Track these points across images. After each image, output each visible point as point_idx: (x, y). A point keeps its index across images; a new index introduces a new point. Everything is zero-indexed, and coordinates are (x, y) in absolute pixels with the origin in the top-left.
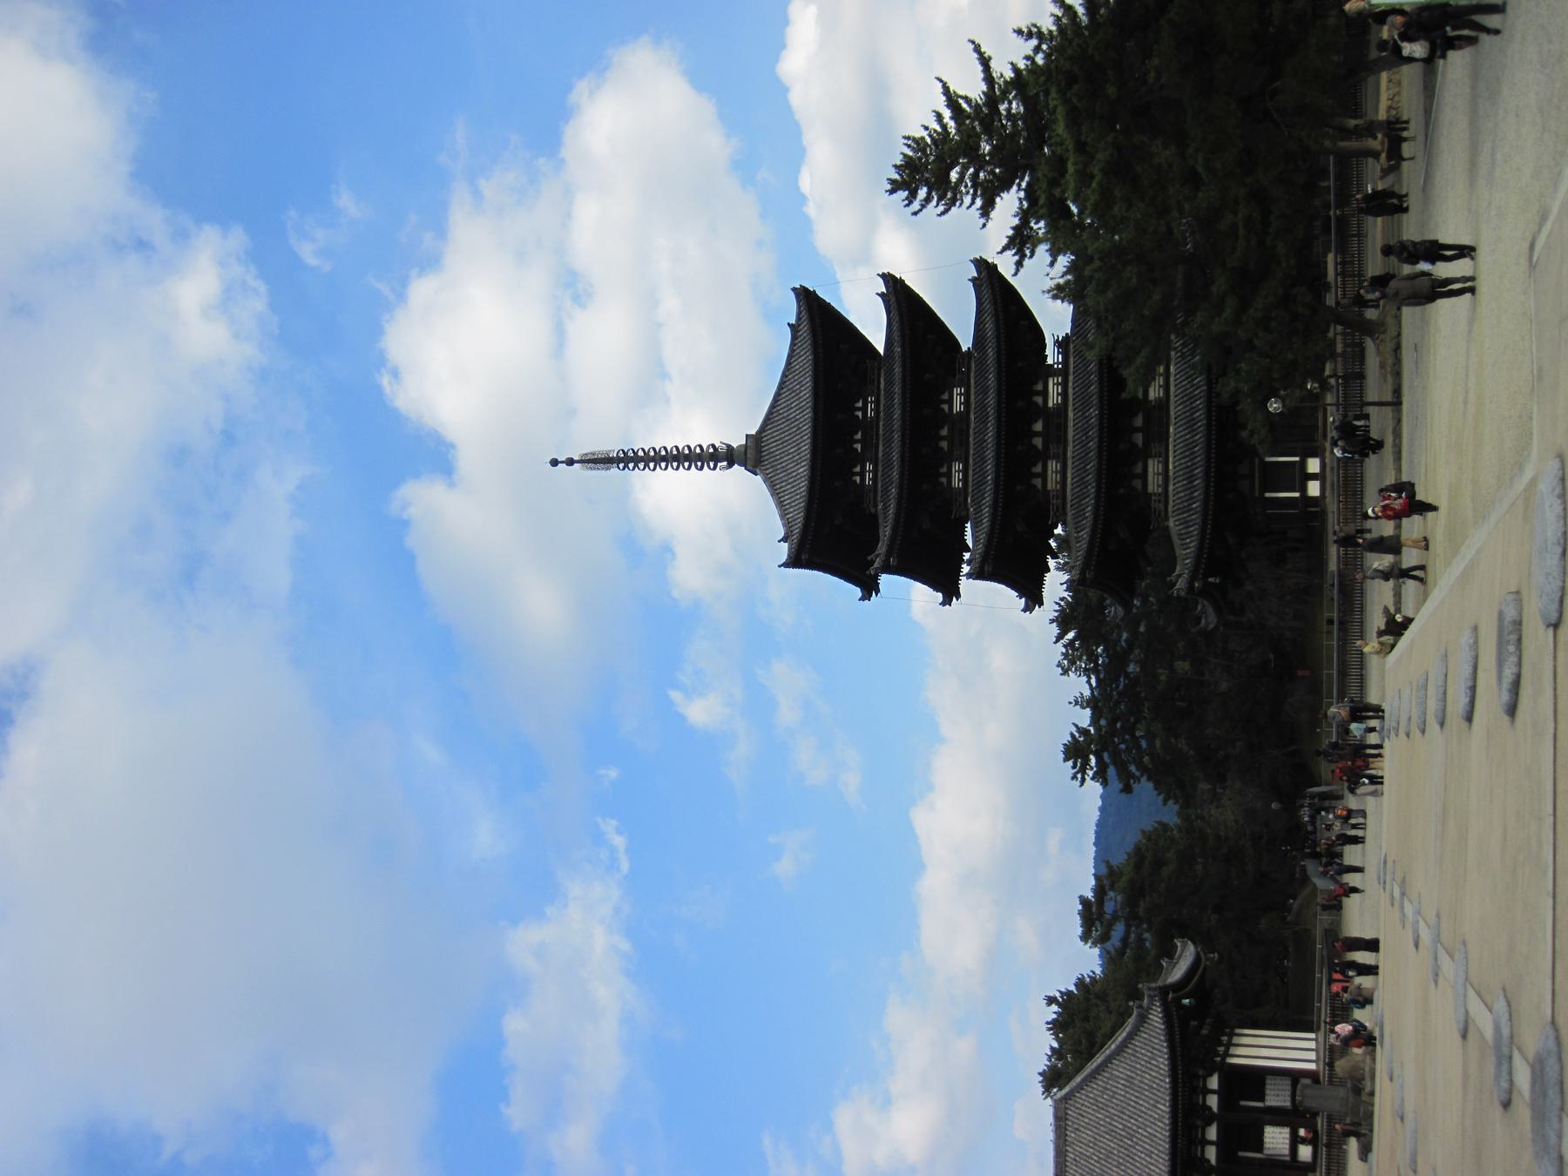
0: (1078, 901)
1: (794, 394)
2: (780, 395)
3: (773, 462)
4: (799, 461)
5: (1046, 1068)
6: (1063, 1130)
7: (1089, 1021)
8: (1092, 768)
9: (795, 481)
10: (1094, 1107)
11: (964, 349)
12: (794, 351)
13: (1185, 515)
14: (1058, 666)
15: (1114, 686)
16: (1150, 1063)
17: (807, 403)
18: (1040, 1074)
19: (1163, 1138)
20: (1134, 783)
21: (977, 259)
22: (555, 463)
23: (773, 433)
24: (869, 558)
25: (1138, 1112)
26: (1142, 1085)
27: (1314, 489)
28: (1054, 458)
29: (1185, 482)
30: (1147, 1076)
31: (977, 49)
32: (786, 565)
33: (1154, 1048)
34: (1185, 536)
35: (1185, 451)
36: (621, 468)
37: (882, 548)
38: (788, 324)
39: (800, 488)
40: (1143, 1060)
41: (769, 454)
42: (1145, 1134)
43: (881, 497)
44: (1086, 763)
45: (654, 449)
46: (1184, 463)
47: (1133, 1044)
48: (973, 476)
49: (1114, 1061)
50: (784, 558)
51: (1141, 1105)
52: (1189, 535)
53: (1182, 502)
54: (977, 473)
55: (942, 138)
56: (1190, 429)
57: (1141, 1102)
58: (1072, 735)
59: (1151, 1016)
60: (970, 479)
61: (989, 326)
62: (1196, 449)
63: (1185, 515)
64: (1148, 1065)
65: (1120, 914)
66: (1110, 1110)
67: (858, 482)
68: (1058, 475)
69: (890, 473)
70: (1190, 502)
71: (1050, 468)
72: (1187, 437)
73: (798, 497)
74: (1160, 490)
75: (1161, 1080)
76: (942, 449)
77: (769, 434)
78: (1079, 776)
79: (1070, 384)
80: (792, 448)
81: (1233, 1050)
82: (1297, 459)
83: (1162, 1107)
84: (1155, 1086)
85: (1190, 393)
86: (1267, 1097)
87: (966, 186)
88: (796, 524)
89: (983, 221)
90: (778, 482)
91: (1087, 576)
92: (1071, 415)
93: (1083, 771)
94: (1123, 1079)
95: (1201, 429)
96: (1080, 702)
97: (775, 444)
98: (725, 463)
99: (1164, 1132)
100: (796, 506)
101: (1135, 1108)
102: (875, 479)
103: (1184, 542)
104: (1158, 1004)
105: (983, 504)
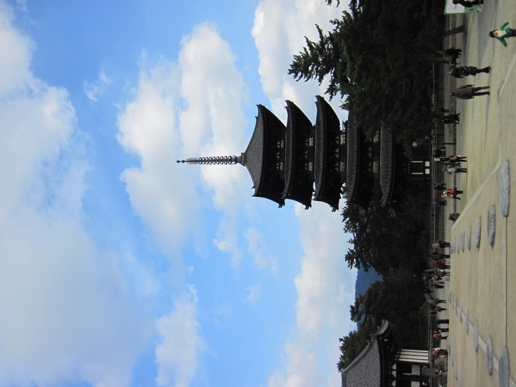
0: (350, 307)
1: (257, 140)
2: (252, 140)
3: (250, 162)
4: (259, 162)
5: (339, 362)
6: (345, 383)
7: (353, 346)
8: (354, 263)
9: (257, 168)
10: (355, 375)
11: (313, 125)
12: (257, 125)
13: (385, 180)
14: (344, 230)
15: (362, 236)
16: (374, 361)
17: (261, 143)
18: (337, 364)
19: (378, 385)
20: (369, 268)
22: (178, 162)
23: (250, 152)
24: (282, 194)
25: (370, 377)
26: (371, 368)
27: (427, 171)
28: (342, 161)
29: (385, 169)
30: (373, 365)
31: (318, 27)
32: (254, 196)
33: (375, 356)
34: (385, 187)
35: (385, 159)
36: (200, 164)
37: (286, 190)
38: (255, 117)
39: (259, 171)
40: (371, 359)
41: (249, 159)
42: (372, 384)
43: (286, 174)
44: (353, 261)
45: (211, 157)
46: (385, 163)
47: (368, 354)
48: (316, 167)
49: (361, 360)
50: (254, 193)
51: (371, 374)
52: (387, 187)
53: (384, 176)
54: (317, 166)
55: (306, 56)
56: (387, 152)
57: (370, 373)
58: (348, 252)
59: (374, 345)
60: (315, 168)
61: (321, 118)
62: (389, 158)
63: (385, 180)
64: (373, 361)
65: (364, 311)
66: (360, 376)
67: (278, 168)
68: (344, 167)
69: (289, 166)
70: (387, 176)
71: (341, 166)
72: (386, 154)
73: (258, 173)
74: (377, 172)
75: (377, 366)
76: (306, 158)
77: (249, 153)
78: (350, 266)
79: (348, 137)
80: (256, 157)
81: (401, 356)
82: (422, 162)
83: (377, 375)
84: (375, 368)
85: (387, 140)
86: (412, 372)
87: (314, 72)
88: (257, 182)
89: (319, 83)
90: (252, 168)
91: (353, 200)
92: (348, 147)
93: (352, 265)
94: (365, 366)
95: (391, 152)
96: (351, 242)
97: (251, 156)
98: (234, 162)
99: (378, 384)
100: (257, 176)
101: (368, 375)
102: (283, 168)
103: (385, 189)
104: (376, 341)
105: (319, 176)
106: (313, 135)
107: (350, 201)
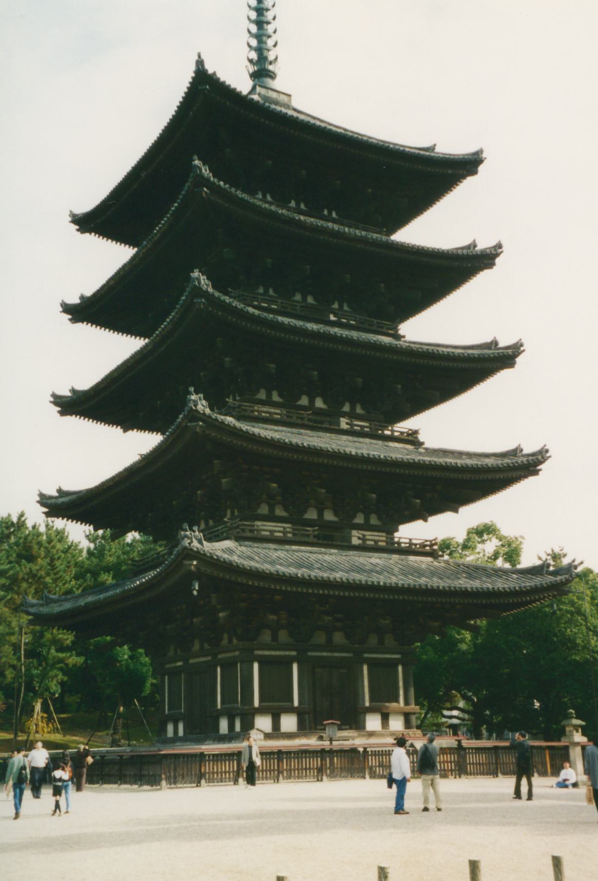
38: (435, 145)
82: (296, 703)
106: (372, 328)
107: (197, 411)
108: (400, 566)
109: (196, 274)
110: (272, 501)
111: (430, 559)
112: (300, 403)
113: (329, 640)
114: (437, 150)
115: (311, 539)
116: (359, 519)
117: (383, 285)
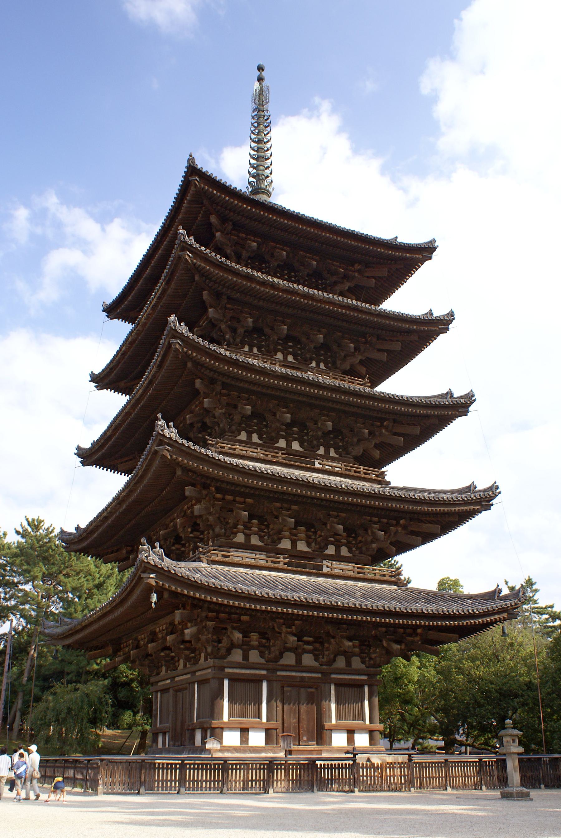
21: (473, 396)
22: (260, 68)
32: (191, 160)
38: (397, 237)
76: (276, 355)
82: (264, 719)
107: (164, 436)
108: (364, 592)
109: (172, 318)
110: (248, 532)
111: (396, 587)
112: (276, 445)
113: (299, 660)
114: (399, 240)
115: (281, 566)
116: (331, 550)
117: (352, 345)
